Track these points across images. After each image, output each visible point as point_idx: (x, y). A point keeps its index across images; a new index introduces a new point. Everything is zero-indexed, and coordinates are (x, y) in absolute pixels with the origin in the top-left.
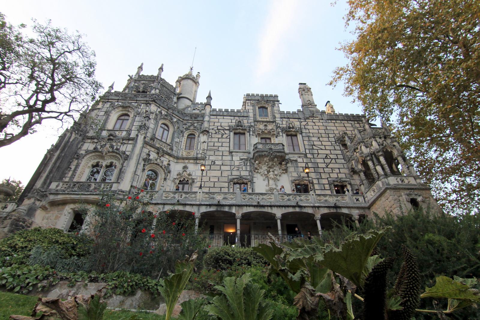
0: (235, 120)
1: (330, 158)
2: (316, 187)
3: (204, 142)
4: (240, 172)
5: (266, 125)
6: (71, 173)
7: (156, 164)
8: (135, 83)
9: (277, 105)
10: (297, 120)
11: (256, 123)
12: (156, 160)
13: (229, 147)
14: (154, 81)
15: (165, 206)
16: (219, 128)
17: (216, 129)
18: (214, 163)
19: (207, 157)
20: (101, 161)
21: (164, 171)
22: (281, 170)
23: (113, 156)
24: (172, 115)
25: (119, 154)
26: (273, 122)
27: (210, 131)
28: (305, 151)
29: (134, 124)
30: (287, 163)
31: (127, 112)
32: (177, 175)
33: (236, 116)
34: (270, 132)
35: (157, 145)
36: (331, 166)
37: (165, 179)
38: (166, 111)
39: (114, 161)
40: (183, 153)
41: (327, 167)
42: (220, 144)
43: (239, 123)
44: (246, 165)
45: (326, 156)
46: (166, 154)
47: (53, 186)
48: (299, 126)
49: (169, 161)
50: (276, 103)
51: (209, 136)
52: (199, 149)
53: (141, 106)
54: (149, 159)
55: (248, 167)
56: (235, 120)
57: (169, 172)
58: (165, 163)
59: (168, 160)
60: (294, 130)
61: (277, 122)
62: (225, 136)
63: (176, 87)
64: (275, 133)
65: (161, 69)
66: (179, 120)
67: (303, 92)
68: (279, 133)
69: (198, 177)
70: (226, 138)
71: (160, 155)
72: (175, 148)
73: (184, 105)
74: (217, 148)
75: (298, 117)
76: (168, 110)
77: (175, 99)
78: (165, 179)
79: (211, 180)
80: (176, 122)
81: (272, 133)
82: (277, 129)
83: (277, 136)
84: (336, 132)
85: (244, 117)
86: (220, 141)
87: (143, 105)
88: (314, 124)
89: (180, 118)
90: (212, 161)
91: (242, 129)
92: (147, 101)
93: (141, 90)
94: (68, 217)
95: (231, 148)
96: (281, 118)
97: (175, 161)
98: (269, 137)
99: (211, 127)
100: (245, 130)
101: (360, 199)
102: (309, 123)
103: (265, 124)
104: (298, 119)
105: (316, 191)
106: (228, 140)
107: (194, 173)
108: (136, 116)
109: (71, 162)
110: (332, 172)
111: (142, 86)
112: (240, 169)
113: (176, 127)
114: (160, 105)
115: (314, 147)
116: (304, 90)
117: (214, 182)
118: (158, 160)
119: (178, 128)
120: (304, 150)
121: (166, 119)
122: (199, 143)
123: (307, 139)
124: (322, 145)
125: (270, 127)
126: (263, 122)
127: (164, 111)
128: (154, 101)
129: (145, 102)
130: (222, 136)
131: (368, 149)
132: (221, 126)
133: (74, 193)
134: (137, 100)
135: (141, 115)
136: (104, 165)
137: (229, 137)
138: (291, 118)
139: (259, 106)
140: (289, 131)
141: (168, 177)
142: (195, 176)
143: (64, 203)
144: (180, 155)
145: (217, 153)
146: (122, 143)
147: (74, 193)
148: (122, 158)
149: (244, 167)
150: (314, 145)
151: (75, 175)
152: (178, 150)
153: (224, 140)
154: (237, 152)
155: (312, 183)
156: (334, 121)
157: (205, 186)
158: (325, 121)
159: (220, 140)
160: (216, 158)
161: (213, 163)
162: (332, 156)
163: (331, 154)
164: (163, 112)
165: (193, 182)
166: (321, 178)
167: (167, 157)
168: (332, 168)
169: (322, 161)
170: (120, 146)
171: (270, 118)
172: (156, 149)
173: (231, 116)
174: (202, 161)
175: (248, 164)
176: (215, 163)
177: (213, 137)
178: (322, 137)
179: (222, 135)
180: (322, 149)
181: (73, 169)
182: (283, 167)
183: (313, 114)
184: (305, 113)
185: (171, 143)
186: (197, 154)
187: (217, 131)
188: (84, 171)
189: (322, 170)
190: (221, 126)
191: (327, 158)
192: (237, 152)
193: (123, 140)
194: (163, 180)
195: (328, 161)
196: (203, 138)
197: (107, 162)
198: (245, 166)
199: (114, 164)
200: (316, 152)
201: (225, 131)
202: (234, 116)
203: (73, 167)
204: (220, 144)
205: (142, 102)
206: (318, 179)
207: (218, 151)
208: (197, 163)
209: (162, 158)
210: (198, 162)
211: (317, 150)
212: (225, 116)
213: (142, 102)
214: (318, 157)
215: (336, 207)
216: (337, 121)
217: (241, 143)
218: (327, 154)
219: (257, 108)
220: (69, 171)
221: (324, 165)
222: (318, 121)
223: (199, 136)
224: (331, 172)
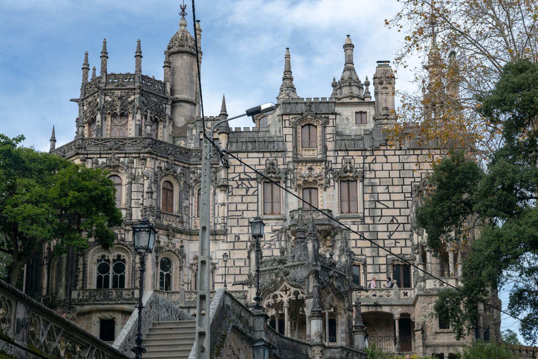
0: (265, 159)
1: (397, 223)
2: (370, 269)
3: (223, 204)
4: (272, 251)
5: (311, 169)
6: (81, 275)
7: (168, 250)
8: (105, 95)
9: (331, 121)
10: (359, 153)
11: (295, 164)
12: (168, 246)
13: (258, 211)
14: (134, 89)
15: (190, 309)
16: (243, 176)
17: (237, 178)
18: (237, 237)
19: (229, 229)
20: (106, 254)
21: (178, 257)
22: (325, 246)
23: (120, 248)
24: (174, 164)
25: (127, 247)
26: (321, 161)
27: (230, 183)
28: (364, 213)
29: (133, 198)
30: (336, 234)
31: (116, 173)
32: (194, 259)
33: (266, 152)
34: (316, 181)
35: (165, 223)
36: (396, 235)
37: (181, 268)
38: (166, 160)
39: (122, 254)
40: (195, 223)
41: (390, 238)
42: (244, 207)
43: (271, 166)
44: (279, 240)
45: (392, 220)
46: (176, 232)
47: (74, 295)
48: (361, 166)
49: (182, 242)
50: (331, 117)
51: (229, 192)
52: (216, 215)
53: (133, 163)
54: (160, 248)
55: (283, 243)
56: (265, 159)
57: (184, 257)
58: (178, 246)
59: (180, 240)
60: (351, 175)
61: (329, 159)
62: (251, 191)
63: (166, 80)
64: (323, 182)
65: (139, 56)
66: (184, 167)
67: (380, 87)
68: (329, 182)
69: (220, 261)
70: (253, 195)
71: (170, 238)
72: (185, 218)
73: (183, 119)
74: (240, 213)
75: (362, 147)
76: (168, 158)
77: (168, 111)
78: (181, 268)
79: (237, 264)
80: (180, 173)
81: (320, 182)
82: (326, 174)
83: (326, 187)
84: (417, 174)
85: (279, 152)
86: (244, 201)
87: (135, 160)
88: (384, 160)
89: (185, 163)
90: (236, 236)
91: (275, 178)
92: (139, 153)
93: (118, 111)
94: (98, 327)
95: (260, 214)
96: (336, 151)
97: (189, 238)
98: (315, 187)
99: (230, 176)
100: (280, 178)
101: (409, 294)
102: (379, 159)
103: (309, 165)
104: (362, 150)
105: (368, 275)
106: (255, 199)
107: (214, 254)
108: (131, 184)
109: (77, 261)
110: (395, 246)
111: (119, 103)
112: (273, 247)
113: (182, 183)
114: (157, 155)
115: (379, 205)
116: (381, 83)
117: (240, 267)
118: (170, 245)
119: (185, 182)
120: (362, 212)
121: (167, 175)
122: (216, 206)
123: (369, 190)
124: (390, 200)
125: (318, 170)
126: (307, 162)
127: (164, 161)
128: (151, 153)
129: (137, 155)
130: (247, 192)
131: (420, 237)
132: (245, 173)
133: (98, 302)
134: (126, 153)
135: (137, 181)
136: (111, 260)
137: (256, 193)
138: (351, 150)
139: (303, 124)
140: (344, 177)
141: (184, 265)
142: (216, 259)
143: (90, 312)
144: (193, 227)
145: (241, 222)
146: (125, 230)
147: (98, 302)
148: (130, 251)
149: (277, 243)
150: (378, 201)
151: (87, 277)
152: (189, 218)
153: (249, 199)
154: (268, 219)
155: (365, 265)
156: (418, 152)
157: (229, 273)
158: (403, 152)
159: (244, 198)
160: (241, 230)
161: (237, 238)
162: (401, 220)
163: (400, 216)
164: (163, 165)
165: (215, 268)
166: (378, 256)
167: (178, 236)
168: (395, 240)
169: (384, 228)
170: (125, 234)
171: (316, 154)
172: (165, 230)
173: (259, 152)
174: (222, 237)
175: (283, 239)
176: (239, 238)
177: (234, 194)
178: (393, 185)
179: (247, 189)
180: (388, 208)
181: (81, 270)
182: (328, 243)
183: (387, 140)
184: (374, 137)
185: (179, 212)
186: (215, 224)
187: (240, 183)
188: (92, 269)
189: (381, 244)
190: (245, 173)
191: (393, 223)
192: (268, 219)
193: (126, 225)
194: (178, 269)
195: (392, 227)
196: (221, 197)
197: (113, 255)
198: (278, 241)
199: (122, 258)
200: (378, 212)
201: (251, 182)
202: (263, 152)
203: (81, 267)
204: (244, 207)
205: (134, 155)
206: (373, 257)
207: (243, 218)
208: (216, 240)
209: (174, 241)
210: (217, 237)
211: (381, 209)
212: (250, 152)
213: (134, 155)
214: (381, 222)
215: (376, 305)
216: (424, 152)
217: (274, 200)
218: (394, 217)
219: (299, 130)
220: (79, 273)
221: (385, 236)
222: (392, 153)
223: (215, 194)
224: (394, 245)
